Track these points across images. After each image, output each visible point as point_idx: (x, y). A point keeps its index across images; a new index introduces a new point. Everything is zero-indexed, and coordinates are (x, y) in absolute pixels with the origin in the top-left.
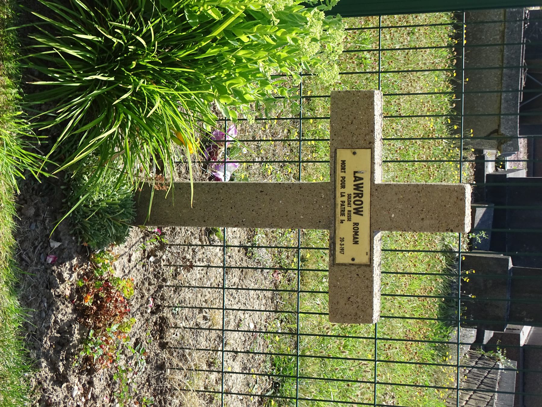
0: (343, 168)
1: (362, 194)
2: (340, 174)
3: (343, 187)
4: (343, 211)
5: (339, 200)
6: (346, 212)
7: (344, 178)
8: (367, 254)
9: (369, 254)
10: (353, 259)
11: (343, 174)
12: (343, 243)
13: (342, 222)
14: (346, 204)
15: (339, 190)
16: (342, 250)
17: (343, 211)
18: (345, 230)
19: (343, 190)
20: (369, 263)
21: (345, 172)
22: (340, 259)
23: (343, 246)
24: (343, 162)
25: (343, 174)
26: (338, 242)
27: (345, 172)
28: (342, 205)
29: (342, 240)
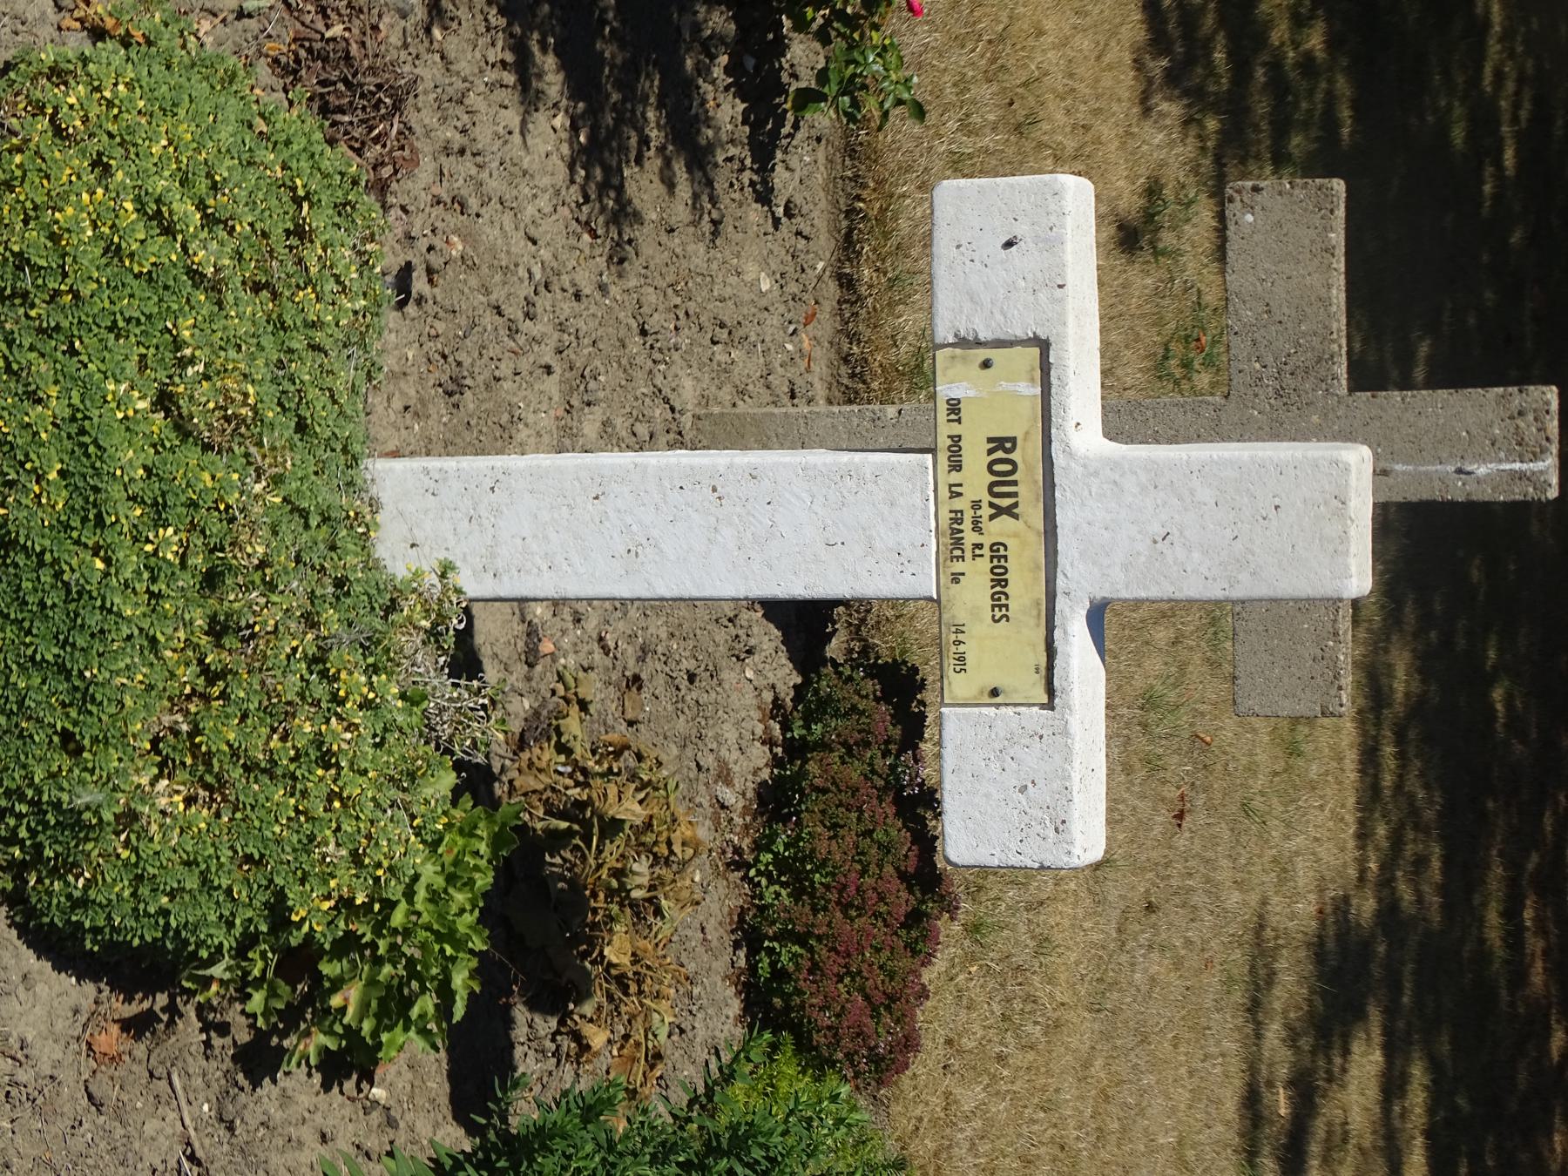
2: (945, 430)
3: (956, 467)
4: (958, 543)
7: (956, 439)
10: (995, 693)
11: (955, 429)
13: (956, 578)
14: (968, 515)
16: (961, 659)
19: (955, 477)
21: (959, 421)
23: (962, 648)
25: (955, 429)
27: (959, 421)
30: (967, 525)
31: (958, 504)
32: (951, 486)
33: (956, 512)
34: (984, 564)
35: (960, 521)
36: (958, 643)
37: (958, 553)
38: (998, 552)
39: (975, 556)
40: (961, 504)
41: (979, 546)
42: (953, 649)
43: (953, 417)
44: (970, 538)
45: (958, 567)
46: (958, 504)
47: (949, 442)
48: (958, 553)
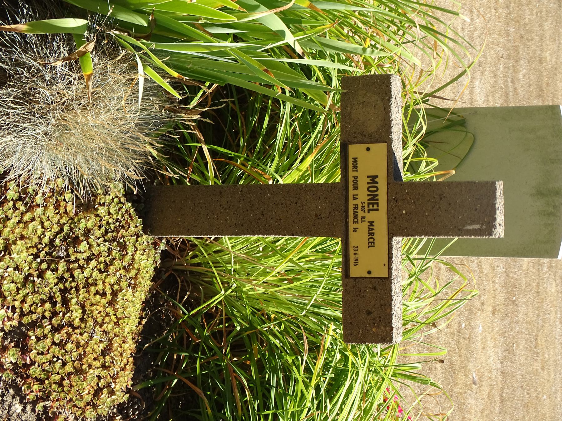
0: (355, 167)
1: (377, 204)
2: (351, 174)
3: (356, 188)
4: (356, 216)
6: (360, 218)
7: (356, 178)
9: (387, 265)
10: (369, 272)
11: (355, 174)
12: (357, 252)
13: (355, 230)
15: (351, 192)
16: (357, 260)
17: (356, 216)
19: (355, 192)
21: (357, 171)
22: (355, 272)
23: (357, 256)
24: (355, 160)
25: (355, 174)
26: (351, 252)
27: (357, 171)
29: (356, 248)
30: (359, 210)
31: (356, 202)
32: (353, 195)
33: (355, 205)
34: (366, 224)
35: (357, 208)
36: (355, 254)
37: (356, 220)
38: (371, 223)
39: (362, 221)
41: (364, 217)
43: (355, 169)
44: (360, 214)
45: (356, 226)
46: (356, 202)
47: (353, 179)
48: (356, 220)
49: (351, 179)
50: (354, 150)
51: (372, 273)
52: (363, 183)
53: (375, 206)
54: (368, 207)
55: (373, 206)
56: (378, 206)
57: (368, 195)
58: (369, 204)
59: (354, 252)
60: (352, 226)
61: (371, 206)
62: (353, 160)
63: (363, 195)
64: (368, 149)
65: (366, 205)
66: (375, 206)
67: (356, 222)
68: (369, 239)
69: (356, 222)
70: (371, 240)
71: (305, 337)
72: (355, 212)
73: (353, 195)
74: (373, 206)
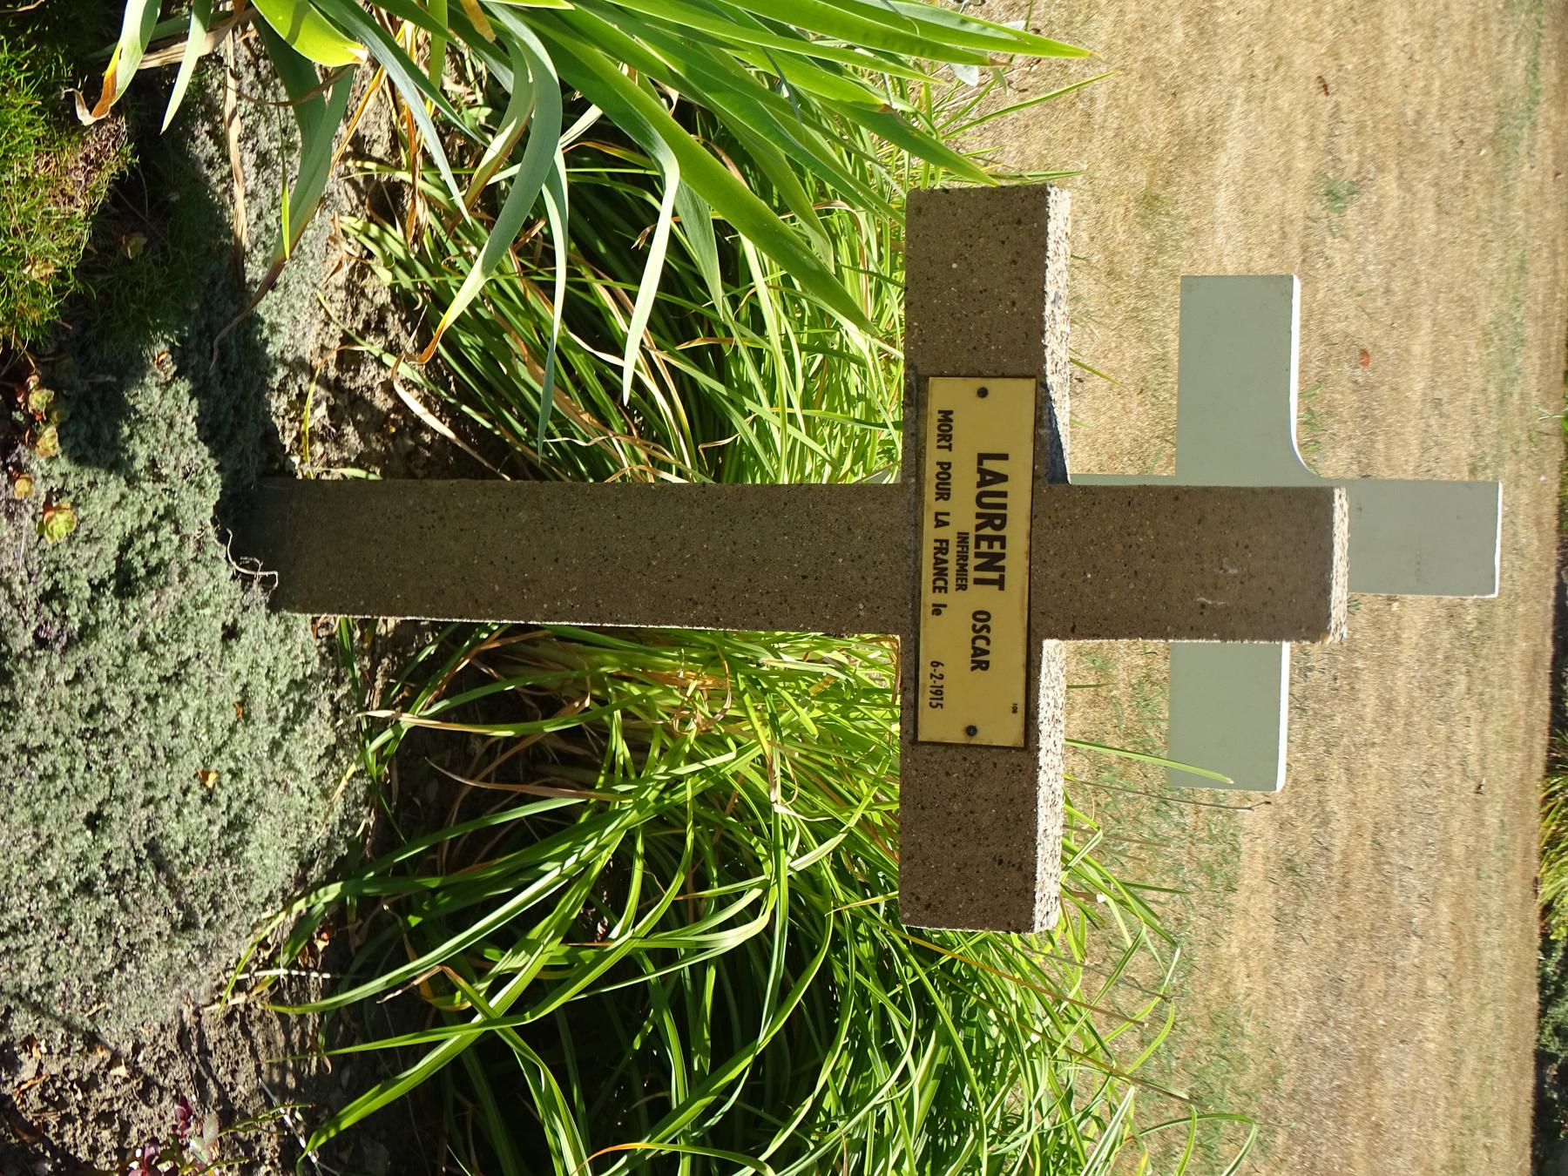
0: (945, 436)
1: (1002, 540)
2: (934, 455)
3: (943, 493)
4: (941, 573)
5: (930, 532)
7: (945, 467)
8: (1015, 711)
10: (971, 731)
11: (944, 456)
12: (940, 670)
13: (937, 610)
16: (938, 692)
17: (941, 573)
18: (944, 638)
19: (942, 506)
20: (1021, 743)
23: (939, 683)
24: (946, 416)
25: (944, 456)
26: (925, 670)
28: (939, 550)
31: (943, 533)
32: (937, 514)
33: (941, 541)
37: (940, 583)
40: (949, 533)
42: (931, 682)
43: (943, 443)
45: (940, 598)
46: (943, 533)
47: (938, 469)
48: (940, 583)
49: (931, 470)
50: (944, 393)
51: (979, 734)
52: (965, 483)
53: (997, 545)
54: (977, 546)
55: (990, 546)
56: (1003, 547)
57: (978, 516)
58: (979, 539)
59: (931, 670)
60: (929, 598)
61: (984, 546)
62: (940, 416)
63: (963, 513)
64: (983, 393)
65: (972, 541)
66: (997, 545)
67: (940, 589)
68: (974, 640)
69: (940, 589)
70: (981, 644)
71: (803, 863)
72: (938, 561)
73: (937, 514)
74: (990, 546)
